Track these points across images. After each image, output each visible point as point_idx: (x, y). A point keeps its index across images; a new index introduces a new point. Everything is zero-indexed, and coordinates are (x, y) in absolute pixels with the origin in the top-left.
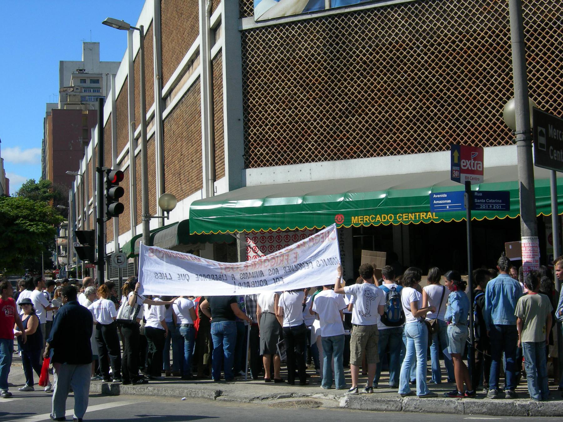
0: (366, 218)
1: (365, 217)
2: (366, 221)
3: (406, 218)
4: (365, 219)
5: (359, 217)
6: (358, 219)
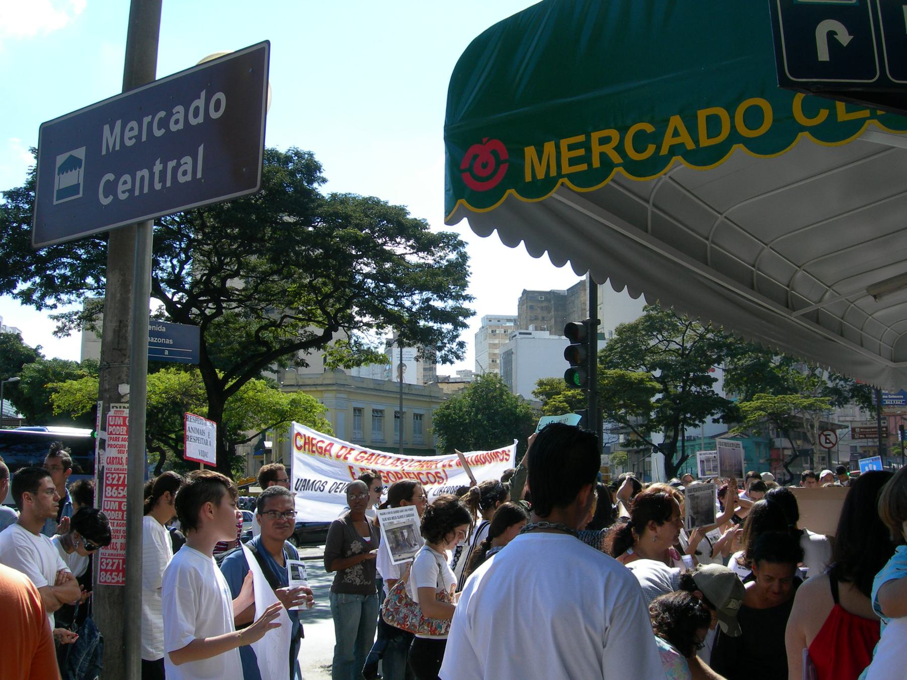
0: (604, 141)
1: (596, 136)
2: (603, 156)
4: (596, 149)
5: (564, 143)
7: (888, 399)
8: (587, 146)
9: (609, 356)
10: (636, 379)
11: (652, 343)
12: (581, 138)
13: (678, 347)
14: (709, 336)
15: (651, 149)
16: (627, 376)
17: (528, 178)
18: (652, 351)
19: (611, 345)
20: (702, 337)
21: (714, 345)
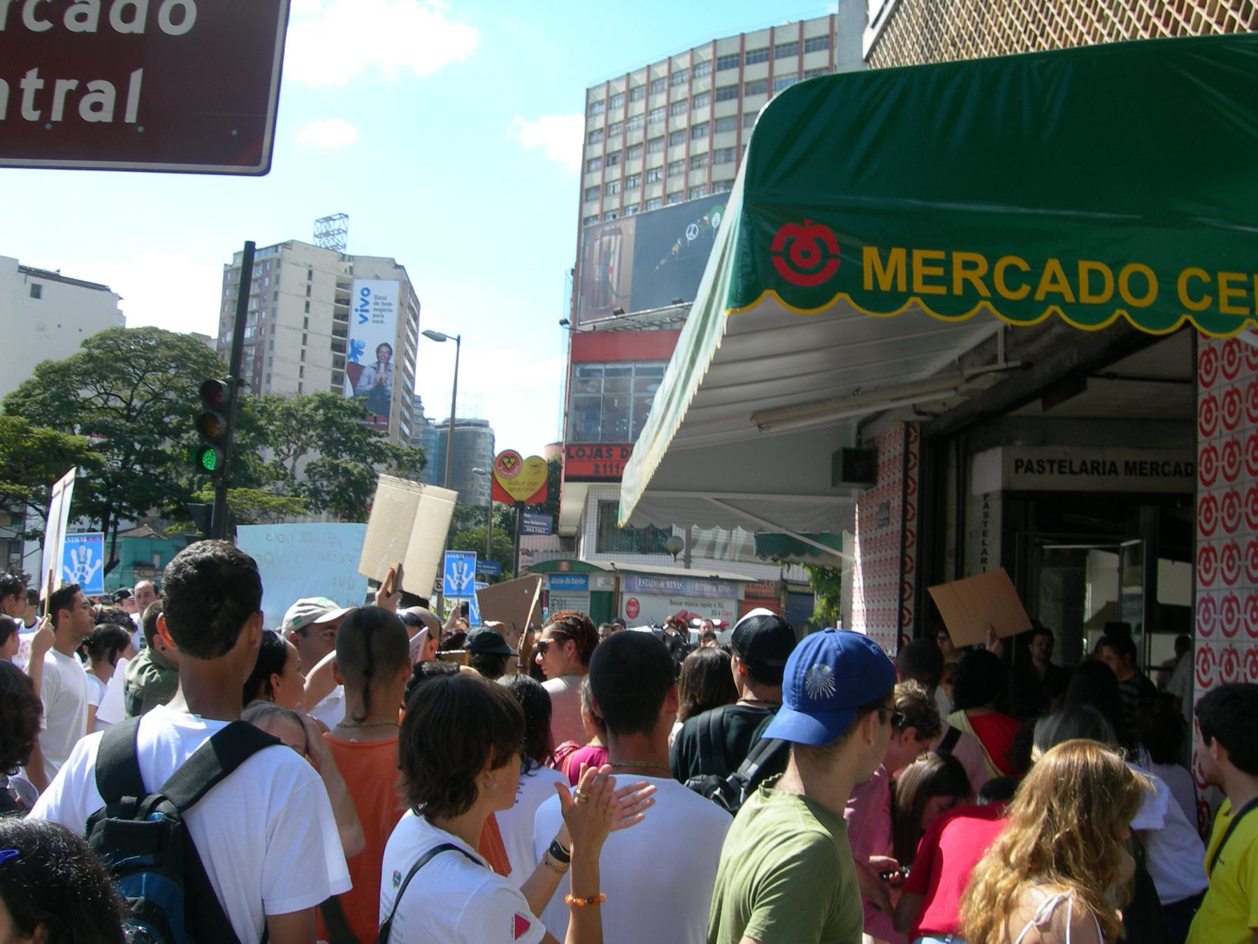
1: (958, 257)
2: (967, 283)
3: (1232, 301)
4: (959, 274)
5: (918, 255)
6: (909, 266)
7: (530, 525)
8: (947, 264)
9: (23, 405)
10: (75, 445)
11: (86, 393)
12: (940, 255)
13: (123, 405)
14: (172, 395)
15: (1025, 290)
16: (61, 439)
17: (868, 285)
18: (85, 405)
19: (28, 390)
20: (156, 397)
21: (173, 409)
